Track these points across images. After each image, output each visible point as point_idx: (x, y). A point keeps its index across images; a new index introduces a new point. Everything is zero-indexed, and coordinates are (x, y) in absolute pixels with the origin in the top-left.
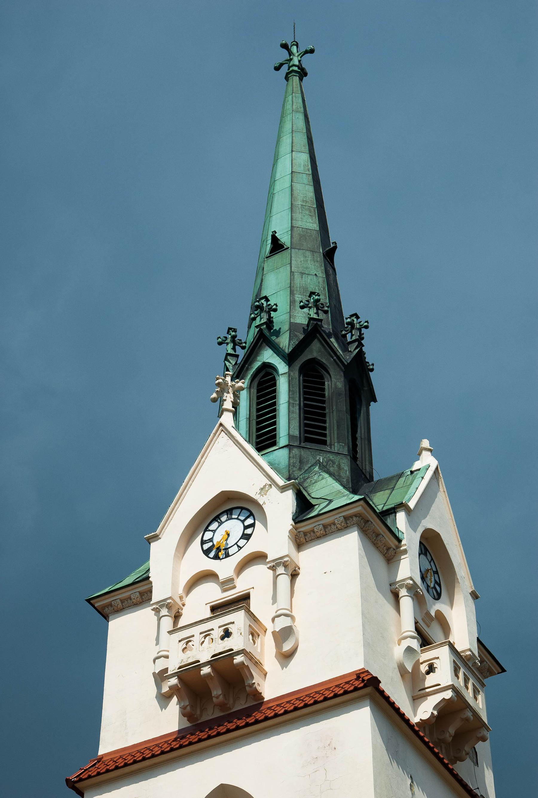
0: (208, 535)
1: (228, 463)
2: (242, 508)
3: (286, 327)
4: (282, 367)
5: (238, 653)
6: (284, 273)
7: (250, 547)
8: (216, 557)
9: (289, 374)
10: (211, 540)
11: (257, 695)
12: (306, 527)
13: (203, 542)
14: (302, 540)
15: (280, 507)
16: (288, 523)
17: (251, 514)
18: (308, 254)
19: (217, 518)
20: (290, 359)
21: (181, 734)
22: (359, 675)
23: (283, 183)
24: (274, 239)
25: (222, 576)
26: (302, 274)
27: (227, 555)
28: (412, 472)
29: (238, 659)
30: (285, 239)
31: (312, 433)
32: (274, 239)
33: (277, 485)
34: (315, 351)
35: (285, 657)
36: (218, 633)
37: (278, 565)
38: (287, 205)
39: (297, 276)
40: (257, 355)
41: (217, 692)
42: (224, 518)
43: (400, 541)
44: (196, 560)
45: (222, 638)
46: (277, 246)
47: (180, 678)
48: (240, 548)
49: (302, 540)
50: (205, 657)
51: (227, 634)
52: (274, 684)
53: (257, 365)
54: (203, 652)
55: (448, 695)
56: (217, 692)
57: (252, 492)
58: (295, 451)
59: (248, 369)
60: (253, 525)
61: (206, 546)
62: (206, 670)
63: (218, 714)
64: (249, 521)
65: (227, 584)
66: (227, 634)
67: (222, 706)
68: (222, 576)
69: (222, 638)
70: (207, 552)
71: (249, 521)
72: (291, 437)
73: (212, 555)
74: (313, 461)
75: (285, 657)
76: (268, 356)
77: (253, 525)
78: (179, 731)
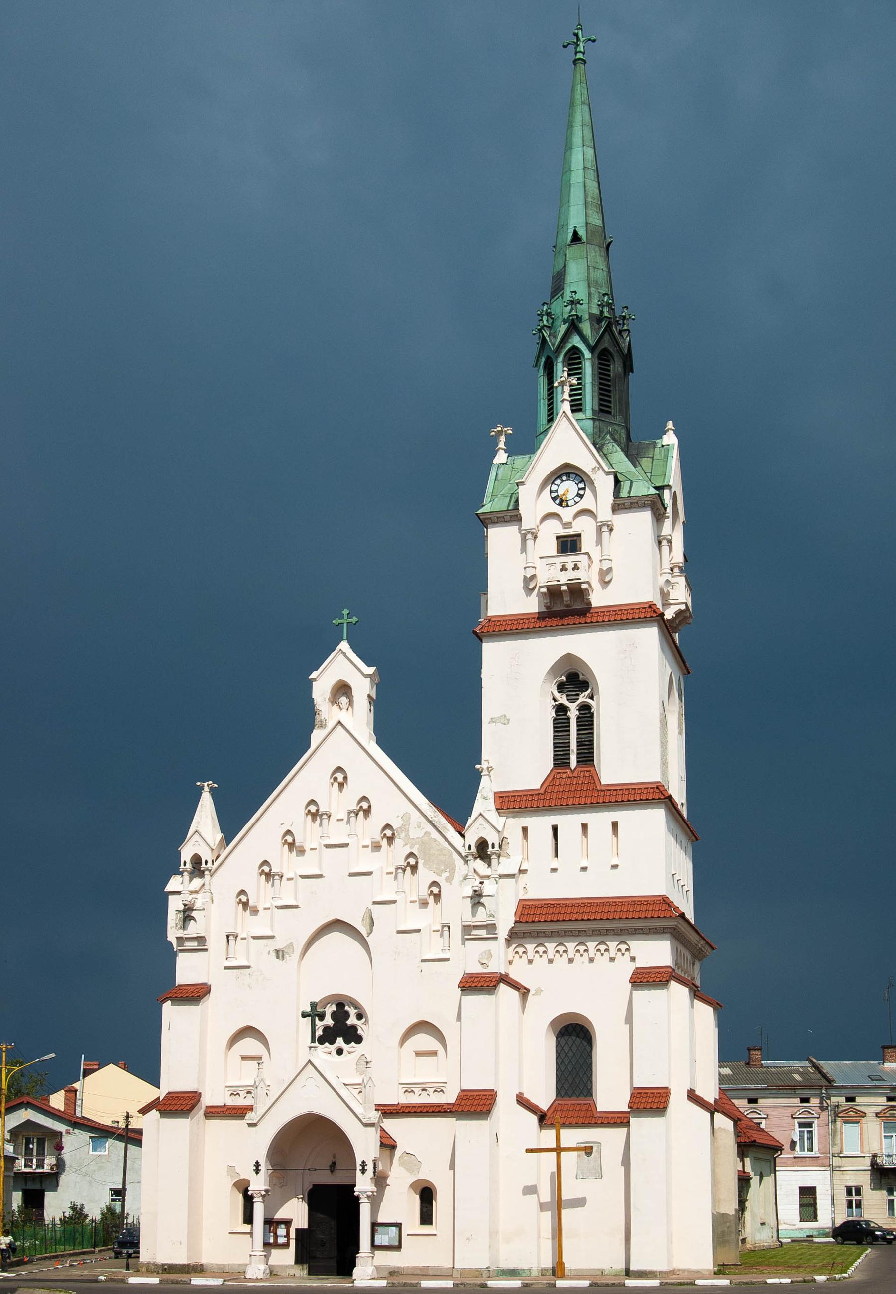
0: (554, 488)
1: (567, 440)
2: (577, 475)
3: (586, 316)
4: (587, 354)
5: (584, 582)
6: (583, 265)
7: (584, 504)
8: (560, 504)
9: (592, 359)
10: (556, 491)
11: (590, 604)
12: (619, 502)
13: (551, 492)
14: (616, 508)
15: (605, 485)
16: (610, 499)
17: (582, 481)
18: (597, 249)
19: (560, 477)
20: (592, 349)
21: (541, 616)
22: (651, 606)
23: (577, 176)
24: (575, 233)
25: (565, 521)
26: (595, 268)
27: (567, 506)
28: (663, 446)
29: (584, 586)
30: (582, 233)
31: (604, 408)
32: (575, 233)
33: (604, 470)
34: (607, 343)
35: (605, 583)
36: (570, 566)
37: (604, 525)
38: (582, 202)
39: (591, 269)
40: (569, 338)
41: (567, 599)
42: (565, 478)
43: (665, 509)
44: (547, 505)
45: (574, 569)
46: (576, 238)
47: (548, 590)
48: (576, 503)
49: (616, 508)
50: (563, 580)
51: (576, 567)
52: (599, 599)
53: (569, 346)
54: (564, 578)
55: (683, 607)
56: (567, 599)
57: (587, 470)
58: (597, 423)
59: (562, 347)
60: (584, 489)
61: (554, 495)
62: (564, 588)
63: (563, 608)
64: (581, 486)
65: (568, 525)
66: (576, 567)
67: (567, 606)
68: (565, 521)
69: (574, 569)
70: (554, 499)
71: (581, 486)
72: (593, 410)
73: (557, 502)
74: (606, 430)
75: (605, 583)
76: (576, 341)
77: (584, 489)
78: (539, 613)
